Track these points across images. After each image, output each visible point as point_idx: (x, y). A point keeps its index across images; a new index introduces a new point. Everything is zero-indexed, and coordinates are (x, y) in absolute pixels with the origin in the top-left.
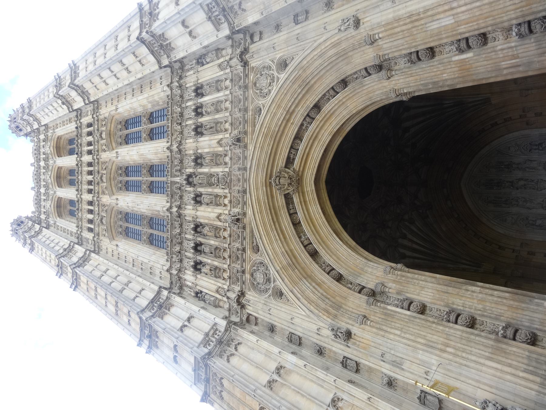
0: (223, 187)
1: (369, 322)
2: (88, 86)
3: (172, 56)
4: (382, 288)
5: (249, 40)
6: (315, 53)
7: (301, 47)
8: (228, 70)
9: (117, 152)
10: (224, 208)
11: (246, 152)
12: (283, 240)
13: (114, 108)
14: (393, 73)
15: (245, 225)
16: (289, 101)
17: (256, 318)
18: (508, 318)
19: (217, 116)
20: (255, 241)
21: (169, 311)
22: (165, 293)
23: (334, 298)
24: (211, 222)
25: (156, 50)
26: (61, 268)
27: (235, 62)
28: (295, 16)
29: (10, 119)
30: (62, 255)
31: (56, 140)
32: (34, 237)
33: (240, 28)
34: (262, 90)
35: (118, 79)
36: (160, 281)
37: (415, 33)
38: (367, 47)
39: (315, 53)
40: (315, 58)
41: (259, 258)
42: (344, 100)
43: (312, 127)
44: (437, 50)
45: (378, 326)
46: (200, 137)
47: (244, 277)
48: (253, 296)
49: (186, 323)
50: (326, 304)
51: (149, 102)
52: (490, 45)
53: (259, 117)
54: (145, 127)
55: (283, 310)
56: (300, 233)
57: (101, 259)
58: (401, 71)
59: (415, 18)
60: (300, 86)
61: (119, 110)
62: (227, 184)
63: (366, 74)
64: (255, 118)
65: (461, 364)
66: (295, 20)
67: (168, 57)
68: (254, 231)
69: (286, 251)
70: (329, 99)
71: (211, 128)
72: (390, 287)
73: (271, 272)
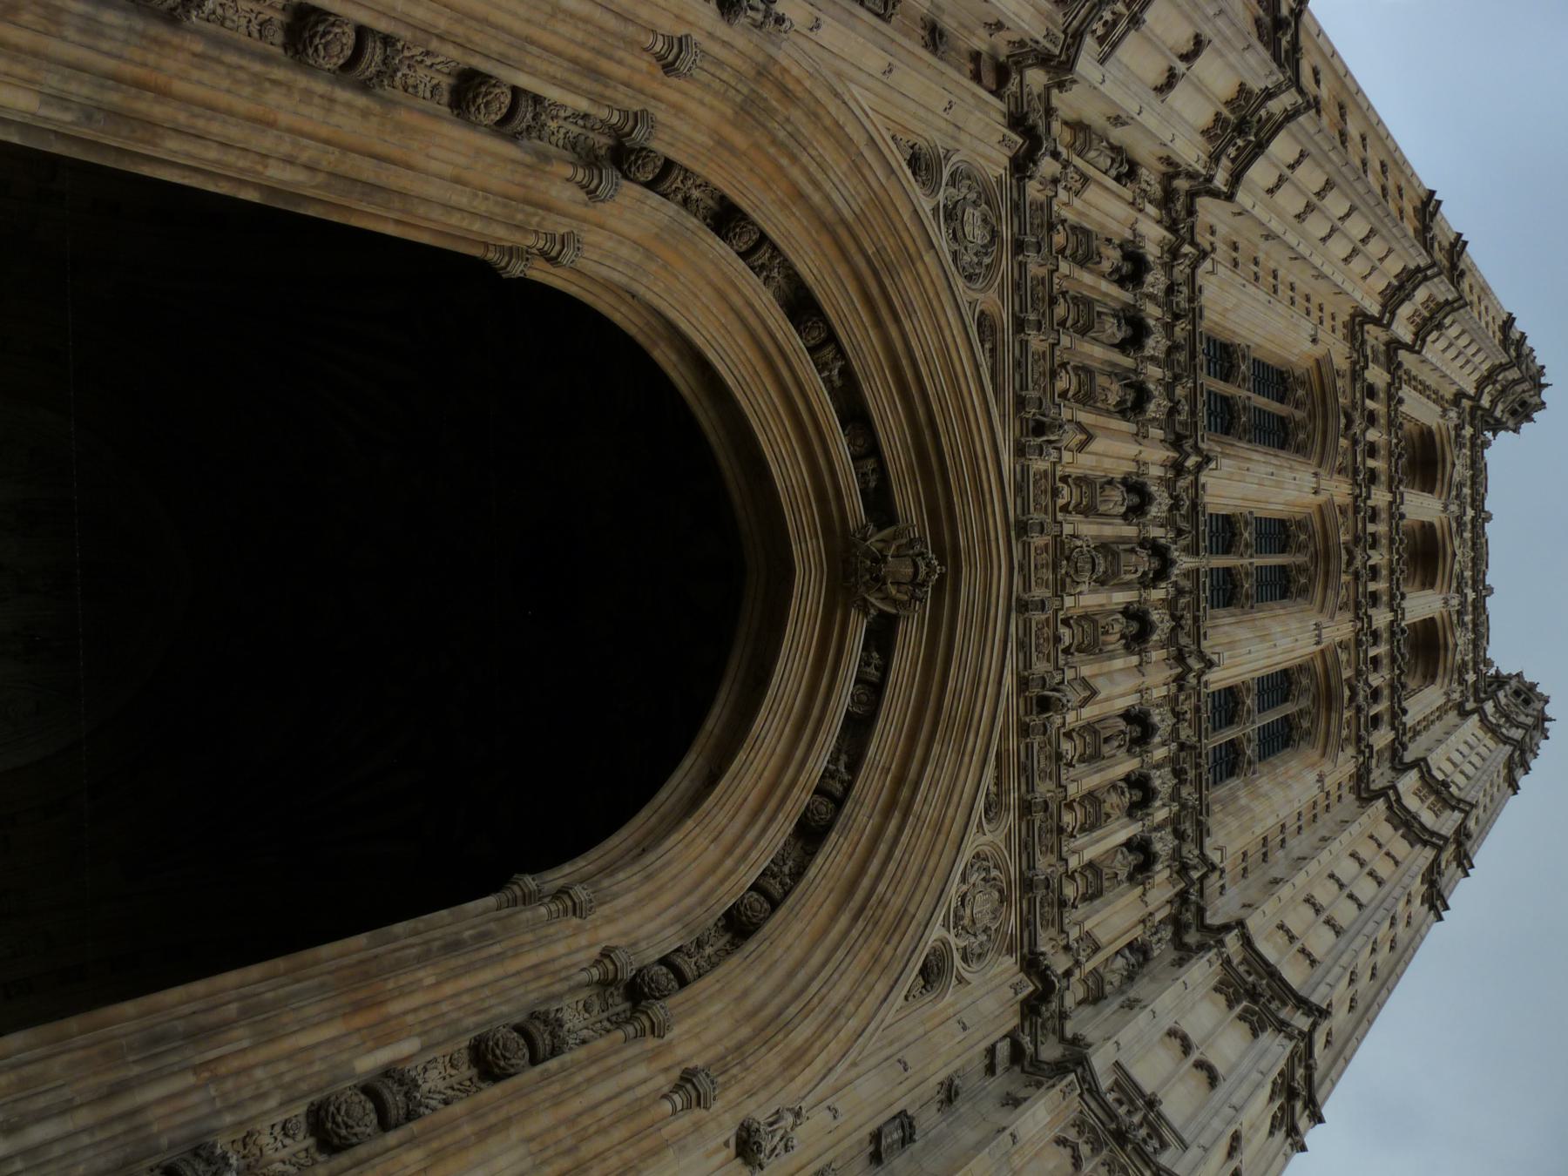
0: (1079, 543)
1: (658, 48)
2: (1400, 847)
3: (1217, 964)
4: (595, 182)
5: (1026, 1040)
6: (853, 1023)
8: (1074, 933)
9: (1318, 643)
10: (1068, 470)
12: (905, 362)
13: (1328, 781)
17: (977, 77)
18: (178, 49)
21: (1218, 114)
22: (1220, 180)
23: (756, 145)
25: (1262, 978)
26: (1454, 266)
27: (1060, 963)
29: (1547, 724)
30: (1448, 308)
31: (1441, 671)
33: (1065, 1082)
35: (1332, 876)
38: (698, 1062)
39: (853, 1023)
40: (851, 1007)
42: (729, 863)
43: (818, 763)
44: (466, 1072)
45: (631, 30)
46: (1133, 706)
49: (1181, 67)
50: (788, 120)
54: (1247, 729)
55: (911, 106)
57: (1358, 295)
61: (1312, 777)
63: (679, 960)
64: (998, 781)
66: (911, 1125)
69: (897, 320)
72: (569, 184)
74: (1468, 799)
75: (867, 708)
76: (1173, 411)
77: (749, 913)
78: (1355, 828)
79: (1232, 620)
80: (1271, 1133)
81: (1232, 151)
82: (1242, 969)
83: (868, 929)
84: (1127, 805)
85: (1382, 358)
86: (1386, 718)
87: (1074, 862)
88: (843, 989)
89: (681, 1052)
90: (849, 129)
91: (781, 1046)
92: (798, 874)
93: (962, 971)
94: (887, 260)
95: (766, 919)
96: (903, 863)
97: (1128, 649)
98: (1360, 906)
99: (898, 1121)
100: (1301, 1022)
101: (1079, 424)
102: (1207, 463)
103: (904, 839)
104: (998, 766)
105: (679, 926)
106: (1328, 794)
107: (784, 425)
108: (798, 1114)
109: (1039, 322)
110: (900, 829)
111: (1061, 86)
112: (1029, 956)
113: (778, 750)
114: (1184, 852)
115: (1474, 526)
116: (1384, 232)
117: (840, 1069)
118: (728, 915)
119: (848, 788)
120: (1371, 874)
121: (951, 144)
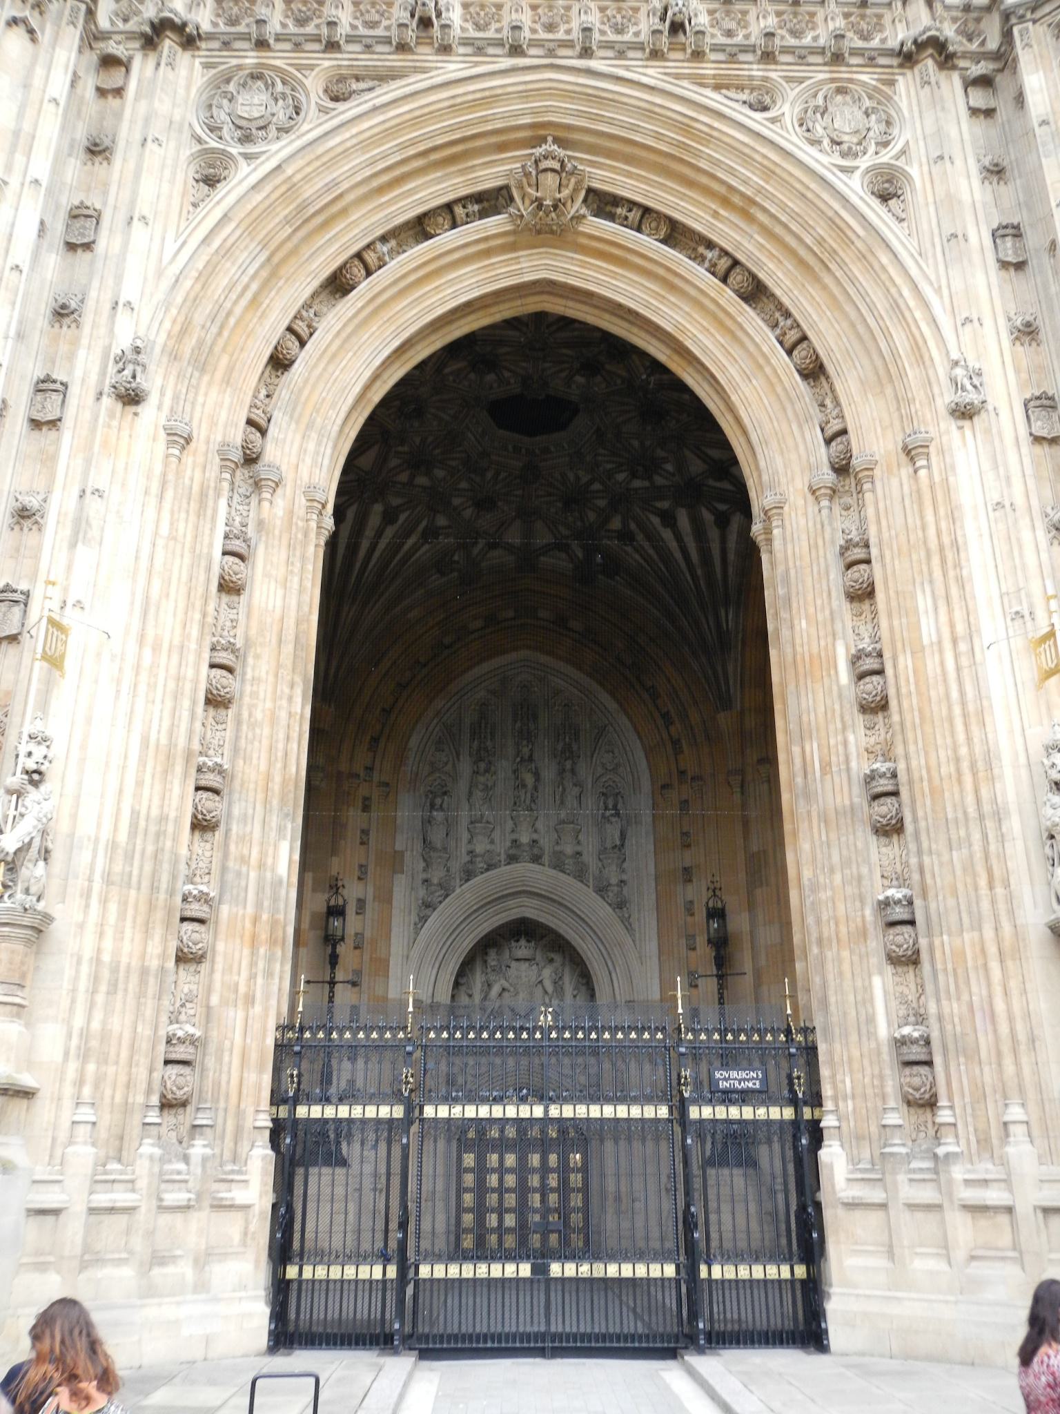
1: (177, 452)
4: (270, 483)
6: (906, 292)
7: (928, 245)
11: (639, 54)
12: (375, 183)
14: (825, 503)
16: (783, 207)
17: (119, 92)
18: (243, 773)
20: (362, 85)
23: (224, 350)
28: (1017, 227)
34: (822, 115)
37: (915, 557)
38: (900, 438)
39: (906, 292)
40: (893, 290)
42: (768, 370)
44: (866, 606)
47: (246, 45)
50: (203, 327)
52: (860, 719)
53: (745, 102)
56: (395, 237)
58: (826, 523)
59: (950, 556)
60: (821, 242)
63: (830, 431)
64: (741, 88)
65: (119, 681)
66: (1006, 227)
68: (394, 84)
69: (341, 196)
70: (774, 326)
73: (274, 147)
90: (200, 265)
108: (956, 363)
110: (765, 210)
113: (687, 309)
121: (186, 134)
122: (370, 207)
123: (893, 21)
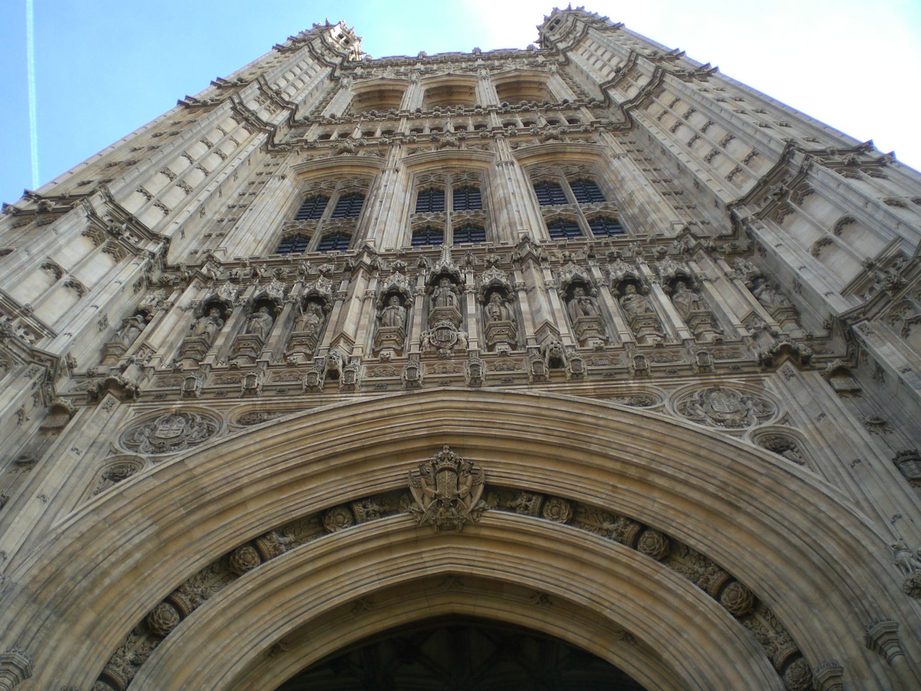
0: (426, 340)
2: (666, 99)
3: (762, 223)
5: (830, 366)
6: (823, 507)
7: (834, 474)
8: (743, 332)
9: (512, 163)
12: (275, 482)
13: (618, 151)
15: (318, 391)
19: (618, 321)
24: (331, 327)
25: (769, 189)
26: (235, 85)
27: (766, 344)
29: (574, 8)
30: (265, 88)
31: (536, 79)
32: (310, 51)
33: (860, 333)
35: (690, 145)
36: (187, 251)
39: (823, 507)
40: (810, 509)
41: (225, 425)
48: (120, 420)
51: (642, 209)
57: (251, 148)
60: (724, 486)
61: (616, 163)
62: (433, 349)
63: (780, 659)
64: (620, 396)
66: (904, 454)
67: (758, 215)
69: (239, 489)
71: (586, 313)
74: (628, 54)
75: (563, 507)
76: (327, 275)
77: (739, 601)
78: (653, 130)
79: (494, 226)
80: (885, 177)
81: (133, 240)
82: (763, 205)
83: (746, 498)
84: (638, 296)
85: (300, 130)
86: (571, 113)
87: (685, 335)
88: (797, 517)
89: (854, 652)
91: (845, 567)
92: (704, 559)
93: (777, 420)
94: (190, 498)
95: (743, 586)
96: (691, 471)
97: (514, 300)
98: (710, 123)
99: (901, 465)
100: (798, 159)
101: (332, 345)
102: (369, 248)
103: (670, 471)
104: (608, 396)
105: (752, 661)
106: (628, 151)
107: (327, 582)
108: (898, 549)
109: (248, 377)
110: (662, 474)
111: (71, 366)
112: (763, 366)
114: (675, 252)
115: (429, 63)
116: (204, 132)
117: (861, 515)
118: (740, 618)
119: (632, 520)
120: (686, 117)
122: (268, 502)
123: (749, 350)
